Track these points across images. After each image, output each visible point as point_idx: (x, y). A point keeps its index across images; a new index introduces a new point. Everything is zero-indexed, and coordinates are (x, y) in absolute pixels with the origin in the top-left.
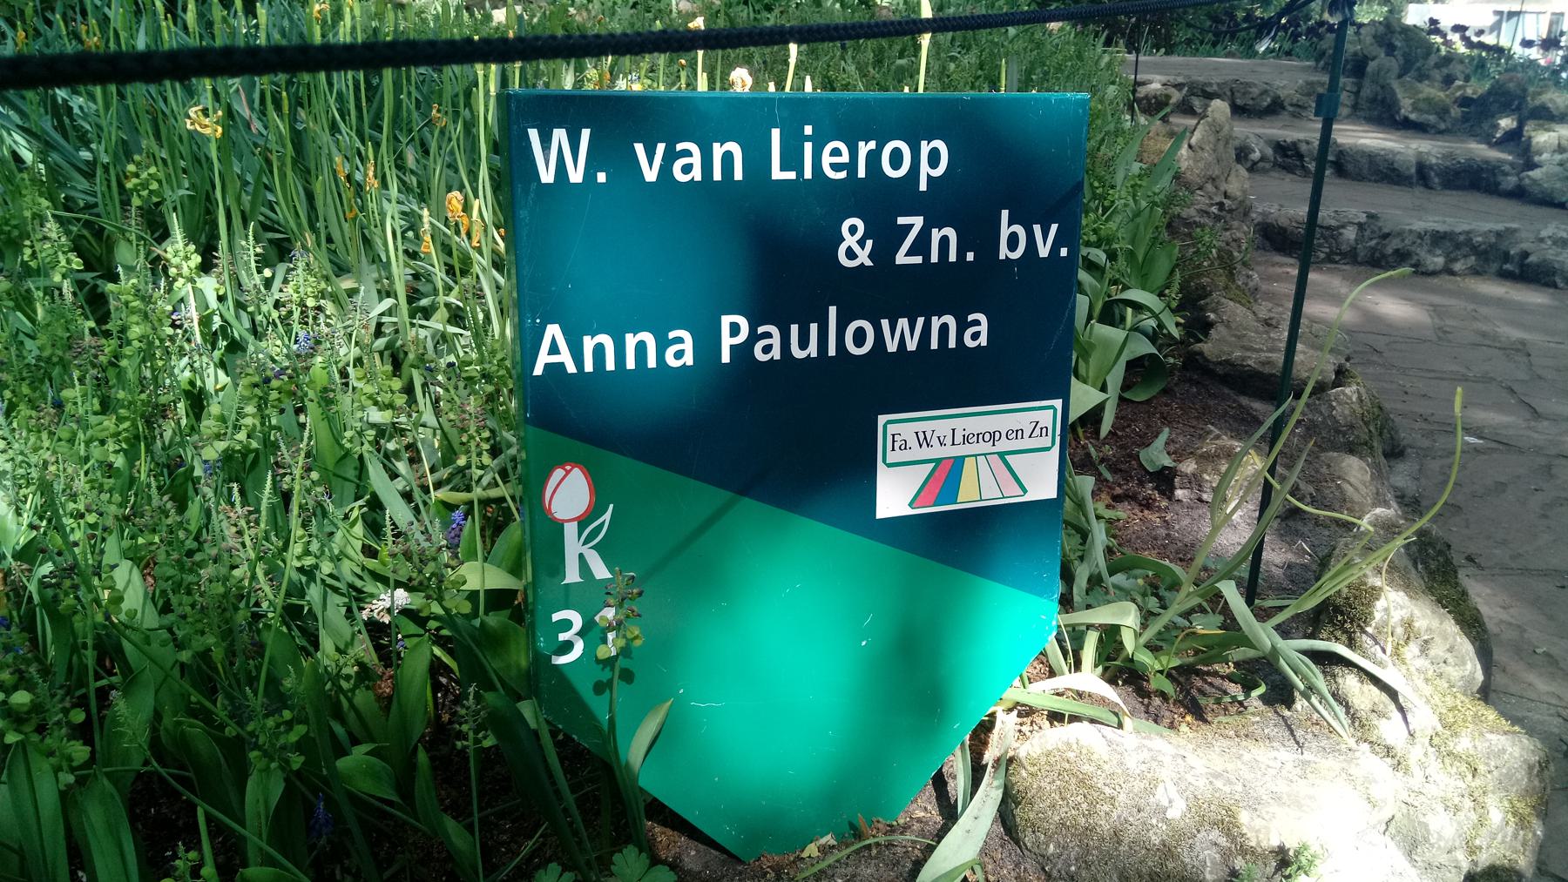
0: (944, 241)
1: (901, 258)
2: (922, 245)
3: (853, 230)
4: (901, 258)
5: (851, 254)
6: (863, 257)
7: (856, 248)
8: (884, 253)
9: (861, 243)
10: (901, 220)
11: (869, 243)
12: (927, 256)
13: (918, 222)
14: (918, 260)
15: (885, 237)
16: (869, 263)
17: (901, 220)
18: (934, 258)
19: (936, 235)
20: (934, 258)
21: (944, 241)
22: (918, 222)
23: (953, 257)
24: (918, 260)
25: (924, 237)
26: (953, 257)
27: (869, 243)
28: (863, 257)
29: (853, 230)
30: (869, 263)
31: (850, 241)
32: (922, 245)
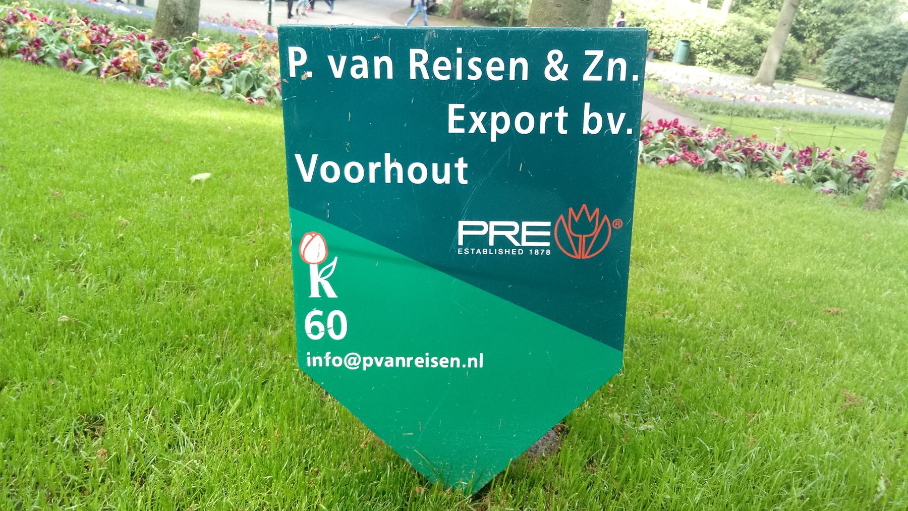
0: (617, 66)
1: (587, 77)
2: (601, 69)
3: (555, 57)
4: (587, 77)
5: (553, 73)
6: (562, 75)
7: (557, 69)
8: (575, 72)
9: (561, 66)
10: (588, 53)
11: (566, 66)
12: (605, 77)
13: (599, 54)
14: (599, 78)
15: (577, 63)
16: (565, 79)
17: (588, 53)
18: (610, 78)
19: (612, 63)
20: (610, 78)
21: (617, 66)
22: (599, 54)
23: (623, 78)
24: (599, 78)
26: (623, 78)
27: (566, 66)
28: (562, 75)
29: (555, 57)
30: (565, 79)
31: (553, 64)
32: (601, 69)
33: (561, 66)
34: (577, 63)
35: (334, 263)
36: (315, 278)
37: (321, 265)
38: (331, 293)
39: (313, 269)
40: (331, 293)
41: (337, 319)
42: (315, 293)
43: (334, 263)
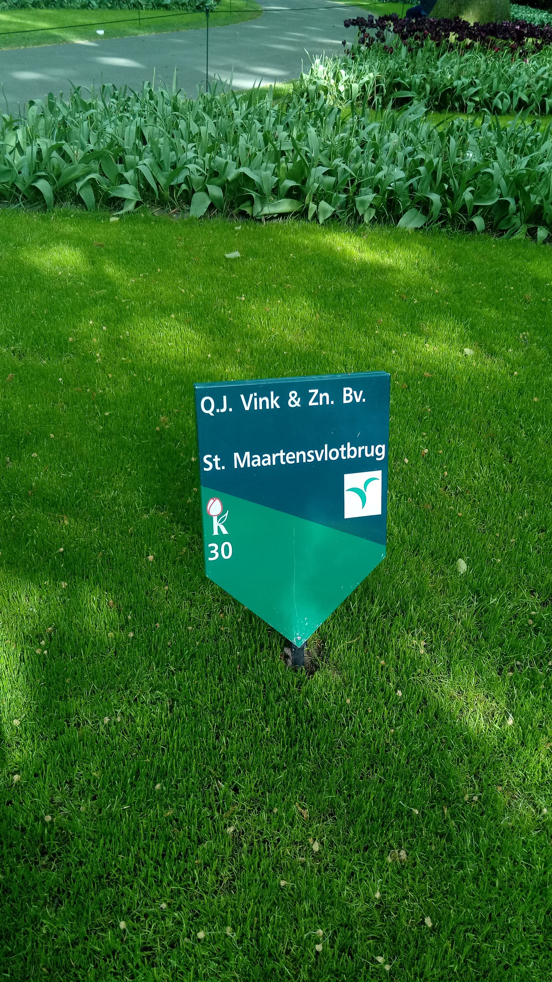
1: (311, 403)
3: (293, 395)
4: (311, 403)
5: (293, 403)
6: (297, 404)
7: (295, 401)
9: (296, 399)
10: (310, 391)
11: (299, 399)
14: (317, 404)
15: (305, 397)
16: (299, 406)
17: (310, 391)
22: (316, 391)
24: (317, 404)
27: (299, 399)
28: (297, 404)
29: (293, 395)
30: (299, 406)
31: (292, 399)
33: (296, 399)
34: (305, 397)
35: (227, 514)
36: (216, 524)
37: (219, 516)
38: (225, 532)
39: (215, 519)
40: (225, 532)
41: (226, 546)
42: (216, 533)
43: (227, 514)
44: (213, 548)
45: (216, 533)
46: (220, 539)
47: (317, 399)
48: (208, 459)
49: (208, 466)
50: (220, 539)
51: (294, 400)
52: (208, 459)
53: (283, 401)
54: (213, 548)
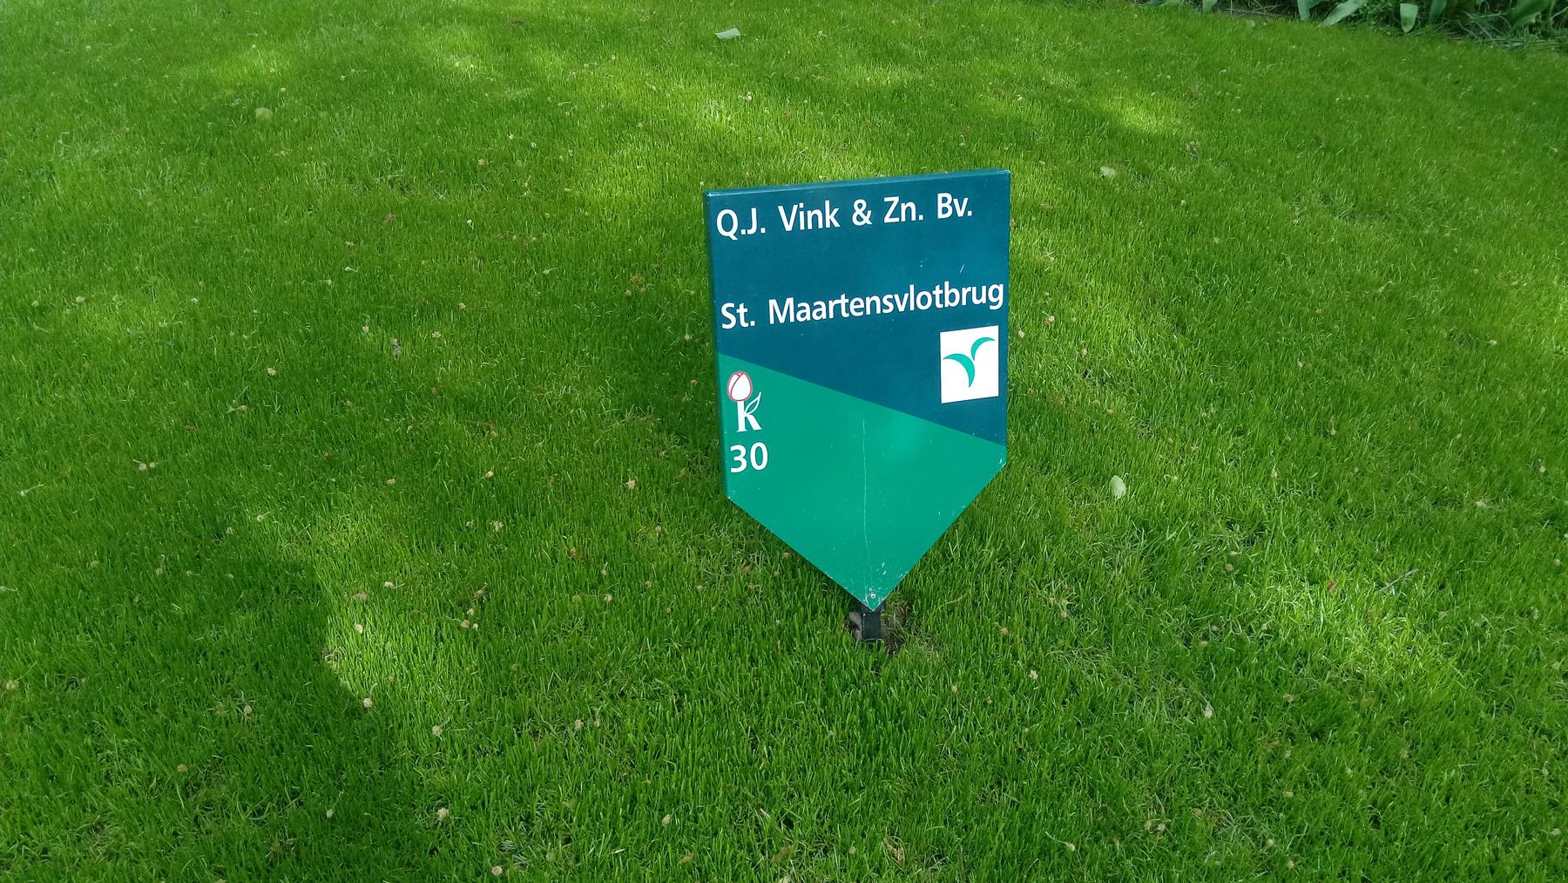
1: (887, 220)
3: (860, 206)
4: (887, 220)
5: (859, 218)
6: (866, 220)
9: (865, 213)
15: (878, 208)
22: (896, 200)
25: (899, 206)
28: (866, 220)
31: (859, 212)
34: (878, 208)
36: (742, 413)
37: (746, 402)
38: (756, 426)
39: (741, 405)
40: (756, 426)
41: (759, 450)
42: (742, 428)
44: (738, 453)
45: (742, 428)
46: (748, 438)
47: (897, 213)
48: (728, 310)
49: (728, 322)
50: (748, 438)
51: (861, 215)
52: (728, 310)
53: (845, 215)
54: (738, 453)
